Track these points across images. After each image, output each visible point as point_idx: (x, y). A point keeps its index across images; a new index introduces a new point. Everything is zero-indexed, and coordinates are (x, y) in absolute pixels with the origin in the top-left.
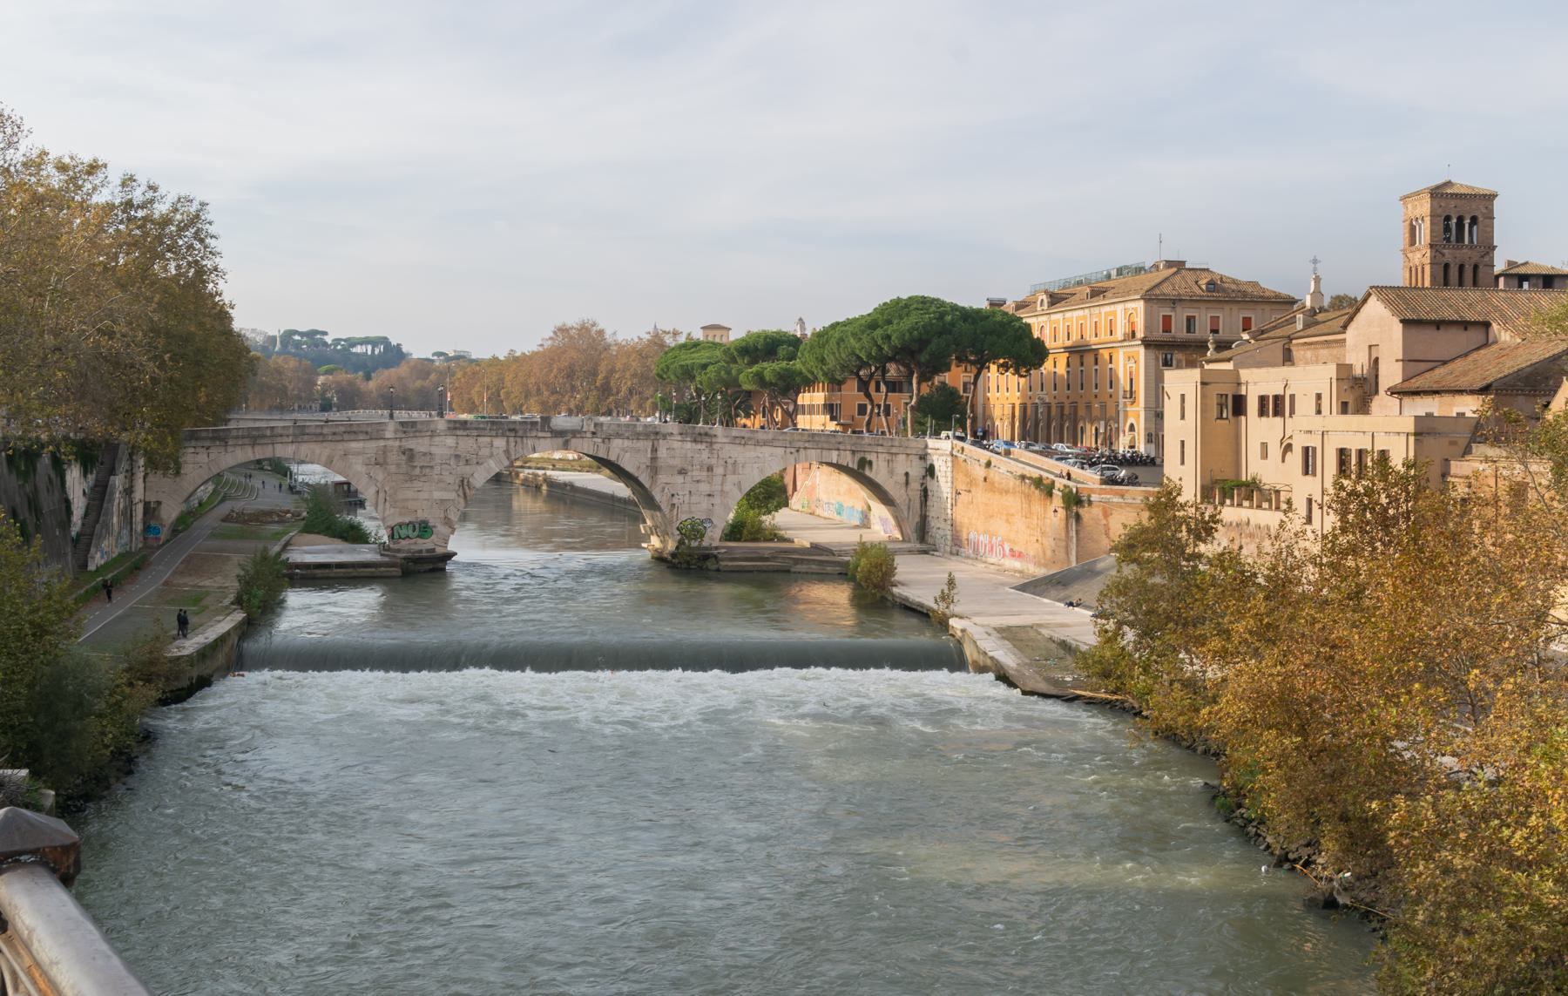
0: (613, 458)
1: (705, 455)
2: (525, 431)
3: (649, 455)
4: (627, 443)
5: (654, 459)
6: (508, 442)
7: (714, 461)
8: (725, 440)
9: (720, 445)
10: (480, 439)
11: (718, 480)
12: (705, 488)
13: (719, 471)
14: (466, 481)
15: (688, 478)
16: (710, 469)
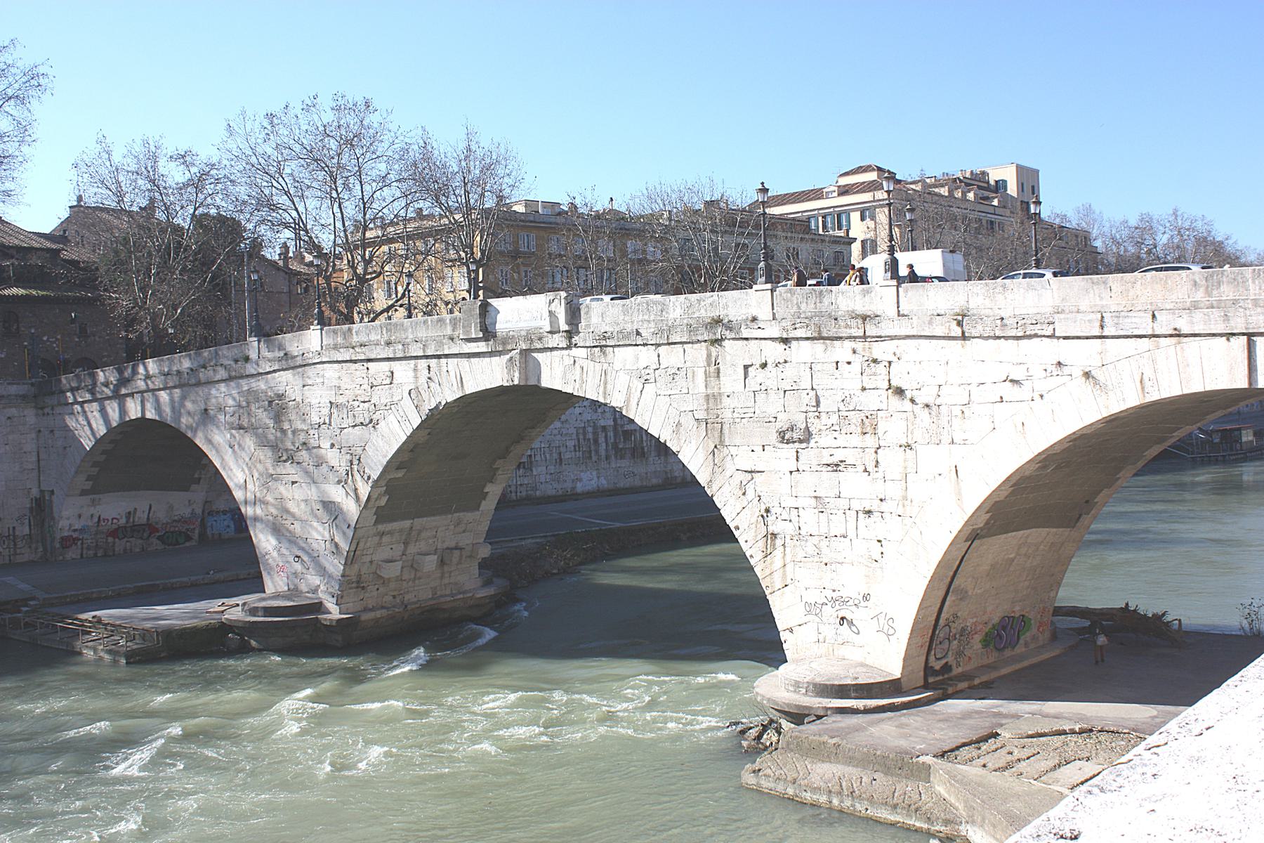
0: (616, 401)
1: (850, 379)
2: (440, 344)
3: (701, 388)
4: (646, 356)
5: (712, 399)
6: (415, 370)
7: (876, 400)
8: (903, 328)
9: (890, 346)
10: (370, 365)
11: (892, 460)
12: (855, 486)
13: (893, 429)
14: (356, 462)
15: (810, 456)
16: (869, 425)
